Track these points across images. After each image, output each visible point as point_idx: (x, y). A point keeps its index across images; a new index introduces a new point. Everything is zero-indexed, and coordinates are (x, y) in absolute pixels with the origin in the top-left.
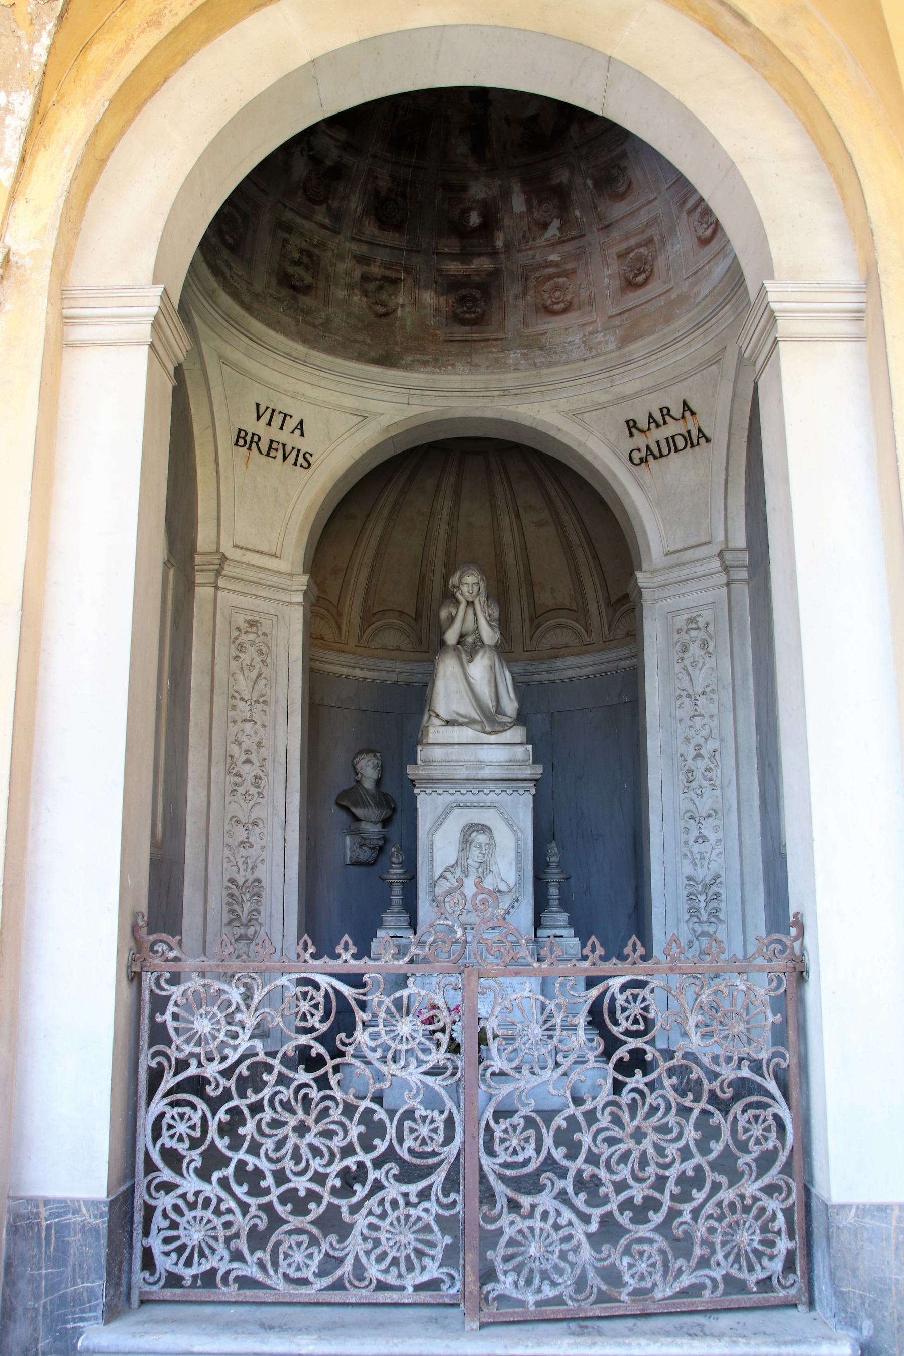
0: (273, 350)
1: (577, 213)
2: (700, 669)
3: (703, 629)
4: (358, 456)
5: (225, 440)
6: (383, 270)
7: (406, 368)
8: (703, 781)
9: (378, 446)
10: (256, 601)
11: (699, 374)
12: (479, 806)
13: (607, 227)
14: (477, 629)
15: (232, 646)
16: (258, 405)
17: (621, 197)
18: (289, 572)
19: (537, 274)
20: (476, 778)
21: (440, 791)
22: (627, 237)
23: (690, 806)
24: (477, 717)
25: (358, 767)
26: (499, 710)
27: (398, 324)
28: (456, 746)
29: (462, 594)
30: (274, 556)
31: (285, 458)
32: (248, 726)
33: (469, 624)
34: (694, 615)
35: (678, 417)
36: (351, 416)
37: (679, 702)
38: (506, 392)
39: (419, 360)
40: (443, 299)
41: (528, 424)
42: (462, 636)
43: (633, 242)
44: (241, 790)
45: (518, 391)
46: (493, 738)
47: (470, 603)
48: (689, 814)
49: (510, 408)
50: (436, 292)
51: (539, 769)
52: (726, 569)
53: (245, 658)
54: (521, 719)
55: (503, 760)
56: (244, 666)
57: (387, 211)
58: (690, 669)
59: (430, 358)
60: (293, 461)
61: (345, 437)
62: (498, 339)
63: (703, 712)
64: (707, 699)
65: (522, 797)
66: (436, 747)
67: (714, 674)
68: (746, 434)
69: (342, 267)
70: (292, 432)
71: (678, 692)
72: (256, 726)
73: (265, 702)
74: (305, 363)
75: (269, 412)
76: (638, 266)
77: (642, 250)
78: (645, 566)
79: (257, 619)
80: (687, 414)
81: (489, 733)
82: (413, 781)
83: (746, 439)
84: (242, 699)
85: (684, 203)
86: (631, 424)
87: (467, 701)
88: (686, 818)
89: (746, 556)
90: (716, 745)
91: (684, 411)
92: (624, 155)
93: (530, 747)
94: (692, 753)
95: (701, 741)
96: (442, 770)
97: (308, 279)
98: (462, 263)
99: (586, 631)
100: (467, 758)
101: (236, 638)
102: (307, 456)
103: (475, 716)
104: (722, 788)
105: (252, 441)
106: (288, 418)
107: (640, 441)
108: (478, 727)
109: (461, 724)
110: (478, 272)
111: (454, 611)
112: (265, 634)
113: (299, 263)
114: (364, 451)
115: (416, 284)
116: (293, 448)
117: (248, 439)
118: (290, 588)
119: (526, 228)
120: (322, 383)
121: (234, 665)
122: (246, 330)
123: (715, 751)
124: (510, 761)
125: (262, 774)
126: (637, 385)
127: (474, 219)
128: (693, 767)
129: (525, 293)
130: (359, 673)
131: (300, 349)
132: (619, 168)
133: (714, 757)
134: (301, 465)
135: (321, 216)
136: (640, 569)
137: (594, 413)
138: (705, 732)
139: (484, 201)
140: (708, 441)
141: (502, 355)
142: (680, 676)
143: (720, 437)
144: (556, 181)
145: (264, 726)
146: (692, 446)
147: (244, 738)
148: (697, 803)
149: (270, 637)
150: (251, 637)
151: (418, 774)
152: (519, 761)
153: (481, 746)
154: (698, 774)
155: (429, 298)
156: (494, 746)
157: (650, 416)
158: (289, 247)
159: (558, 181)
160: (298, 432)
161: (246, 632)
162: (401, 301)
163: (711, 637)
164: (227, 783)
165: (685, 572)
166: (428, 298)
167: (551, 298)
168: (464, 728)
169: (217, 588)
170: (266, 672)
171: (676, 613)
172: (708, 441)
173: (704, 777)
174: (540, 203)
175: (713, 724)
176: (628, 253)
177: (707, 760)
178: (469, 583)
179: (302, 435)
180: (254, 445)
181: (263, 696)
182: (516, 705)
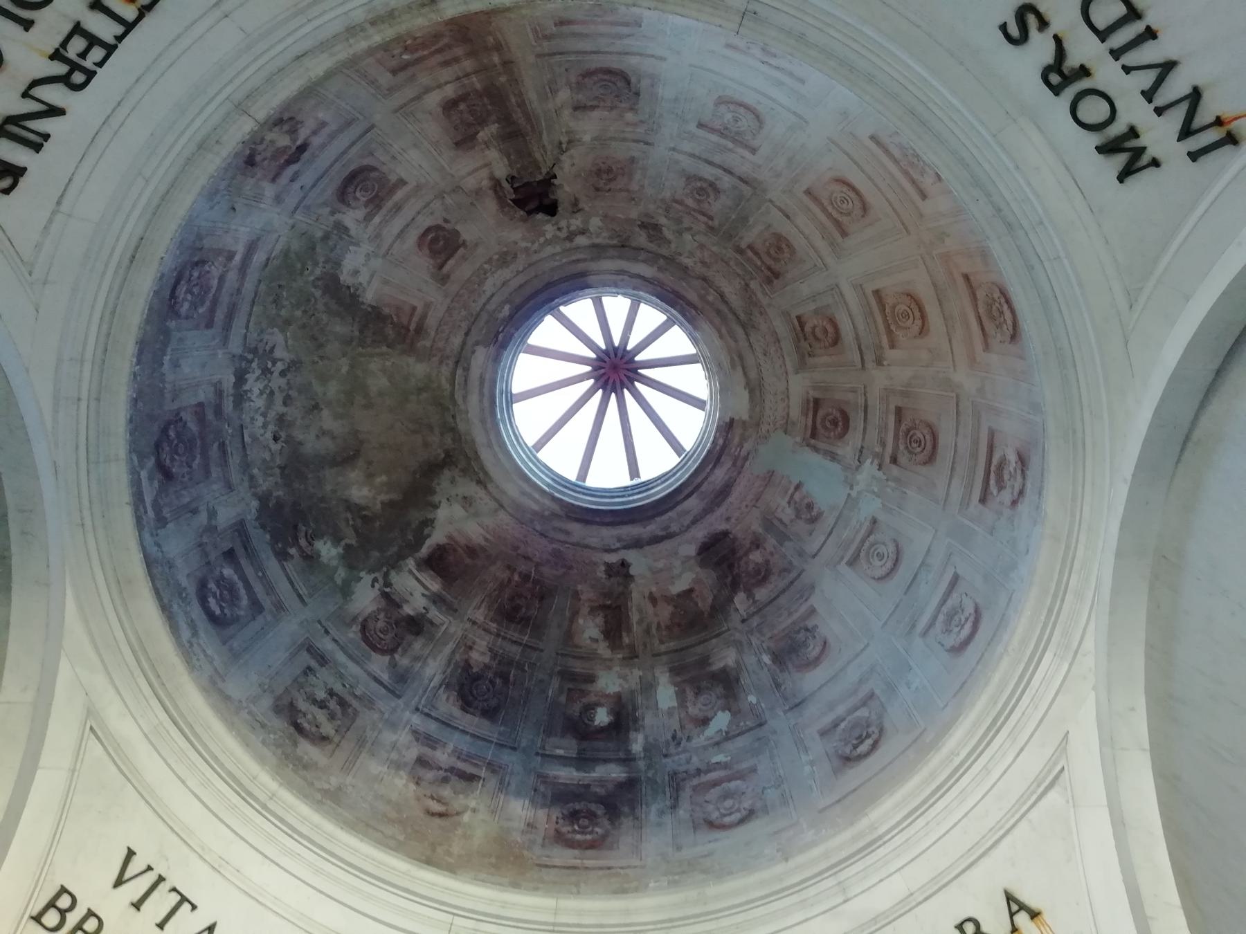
0: (213, 761)
1: (752, 699)
6: (454, 759)
11: (1023, 825)
13: (796, 706)
17: (816, 662)
19: (695, 782)
22: (831, 706)
27: (459, 832)
40: (542, 814)
43: (841, 710)
50: (532, 801)
57: (476, 690)
62: (629, 867)
69: (388, 737)
74: (264, 809)
76: (856, 733)
77: (858, 713)
85: (914, 626)
91: (1012, 915)
92: (812, 611)
97: (328, 729)
98: (578, 769)
106: (186, 906)
110: (601, 782)
113: (322, 705)
115: (503, 786)
119: (676, 726)
120: (285, 861)
122: (169, 696)
127: (602, 717)
129: (674, 807)
131: (265, 781)
132: (807, 630)
135: (379, 664)
139: (618, 697)
144: (717, 666)
155: (519, 810)
158: (312, 679)
159: (721, 665)
162: (473, 804)
166: (519, 809)
167: (718, 809)
174: (697, 694)
176: (836, 726)
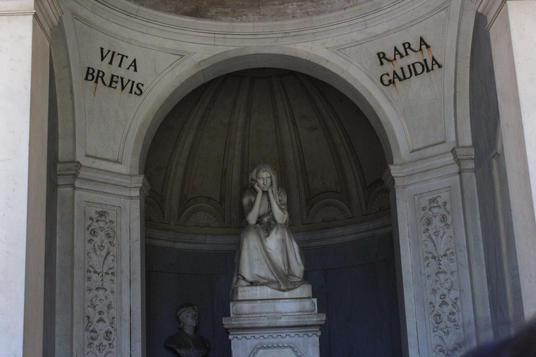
2: (442, 237)
3: (442, 207)
4: (177, 84)
5: (78, 76)
7: (212, 18)
8: (448, 323)
9: (193, 77)
10: (105, 197)
11: (431, 18)
12: (278, 347)
14: (270, 212)
15: (87, 232)
16: (102, 49)
18: (128, 173)
20: (275, 325)
21: (248, 336)
23: (439, 342)
24: (274, 279)
25: (180, 317)
26: (290, 273)
28: (259, 302)
29: (259, 186)
30: (117, 162)
31: (123, 88)
32: (101, 292)
33: (264, 209)
34: (435, 196)
35: (416, 50)
36: (172, 56)
37: (427, 262)
38: (286, 34)
39: (221, 12)
41: (304, 57)
42: (260, 218)
44: (96, 343)
45: (296, 34)
46: (286, 295)
47: (265, 193)
48: (439, 348)
49: (290, 46)
51: (323, 317)
52: (458, 161)
53: (97, 240)
54: (307, 278)
55: (295, 310)
56: (96, 247)
58: (434, 237)
59: (229, 10)
60: (129, 90)
61: (167, 71)
63: (445, 270)
64: (447, 259)
65: (310, 338)
66: (244, 302)
67: (452, 241)
68: (469, 61)
70: (128, 69)
71: (426, 254)
72: (107, 292)
73: (113, 274)
74: (136, 17)
75: (110, 55)
78: (396, 161)
79: (105, 210)
80: (424, 47)
81: (284, 291)
82: (228, 329)
83: (469, 65)
84: (95, 272)
86: (381, 55)
87: (266, 267)
88: (437, 351)
89: (472, 151)
90: (457, 295)
91: (421, 45)
93: (315, 300)
94: (439, 301)
95: (446, 291)
96: (249, 320)
99: (349, 208)
100: (268, 310)
101: (90, 226)
102: (140, 86)
103: (273, 278)
104: (463, 328)
105: (98, 76)
106: (125, 58)
107: (388, 68)
108: (275, 286)
109: (262, 285)
111: (253, 199)
112: (111, 222)
114: (183, 80)
116: (129, 81)
117: (95, 74)
118: (129, 186)
121: (89, 246)
123: (456, 299)
124: (301, 311)
125: (112, 330)
126: (385, 27)
128: (440, 312)
130: (178, 245)
133: (455, 303)
134: (135, 93)
136: (392, 163)
137: (353, 48)
138: (447, 285)
140: (440, 66)
141: (282, 6)
142: (426, 243)
143: (449, 64)
145: (112, 292)
146: (428, 71)
147: (98, 302)
148: (445, 340)
149: (115, 223)
150: (102, 224)
151: (232, 324)
152: (307, 311)
153: (278, 301)
154: (445, 318)
156: (288, 300)
157: (396, 49)
160: (132, 68)
161: (97, 221)
163: (449, 213)
164: (86, 338)
165: (426, 164)
168: (265, 287)
169: (74, 188)
170: (113, 250)
171: (420, 195)
172: (440, 66)
173: (449, 320)
175: (453, 279)
177: (450, 306)
178: (265, 177)
179: (136, 70)
180: (100, 79)
181: (111, 269)
182: (302, 268)
